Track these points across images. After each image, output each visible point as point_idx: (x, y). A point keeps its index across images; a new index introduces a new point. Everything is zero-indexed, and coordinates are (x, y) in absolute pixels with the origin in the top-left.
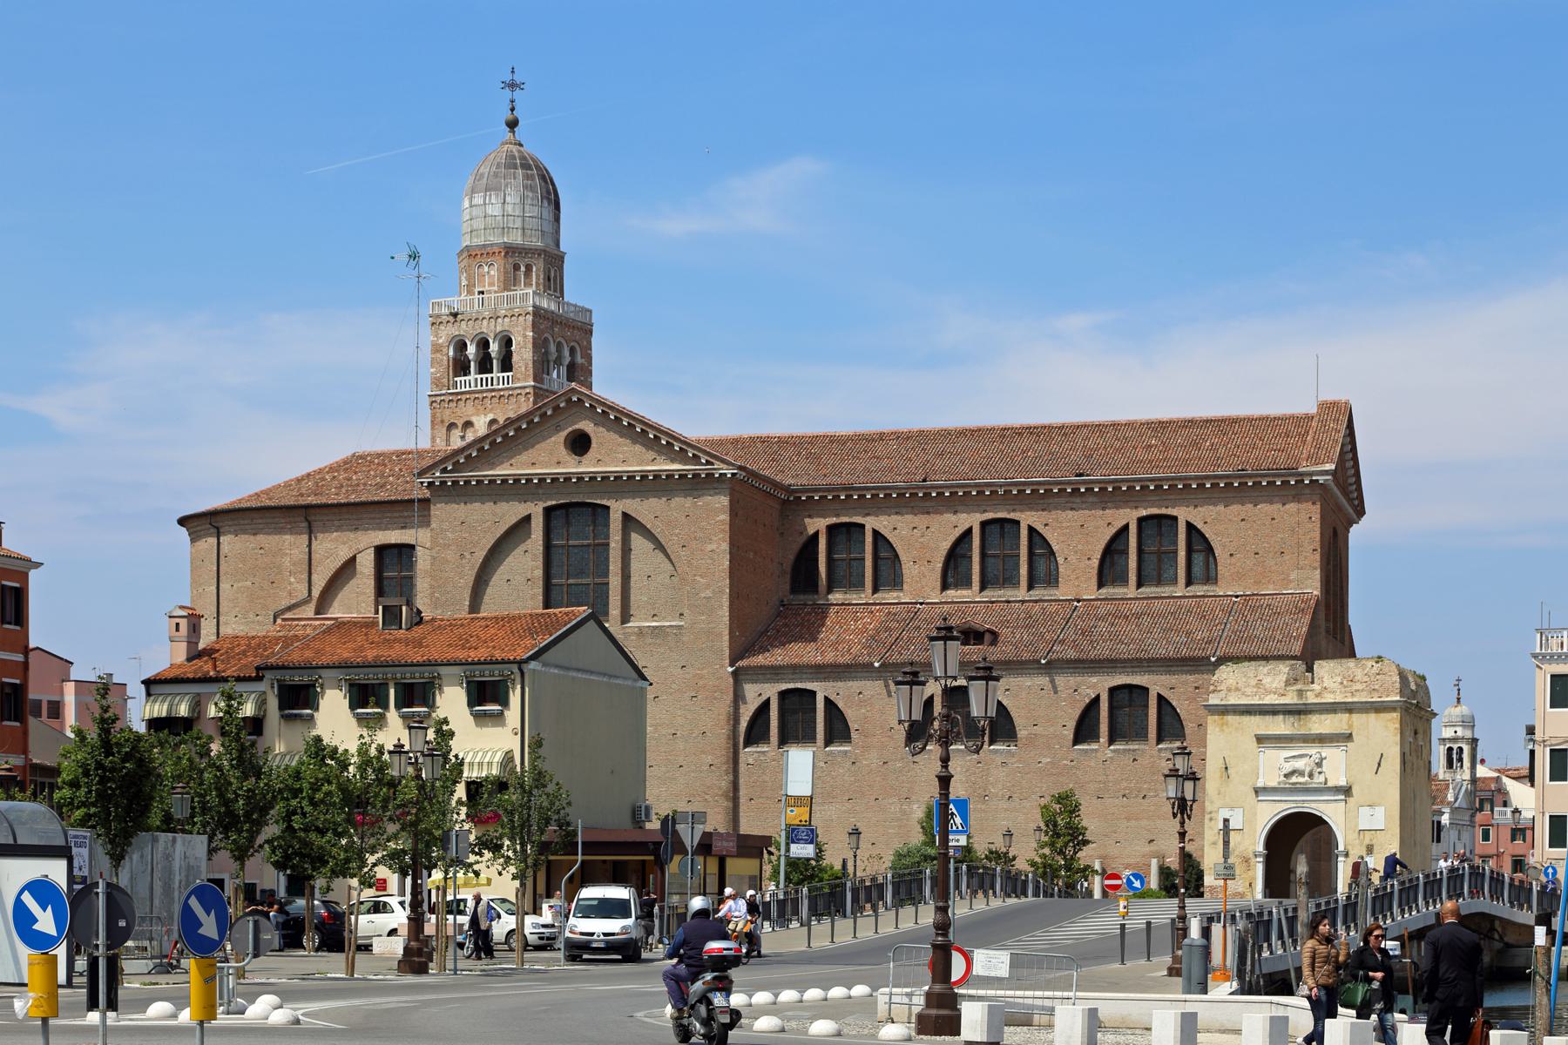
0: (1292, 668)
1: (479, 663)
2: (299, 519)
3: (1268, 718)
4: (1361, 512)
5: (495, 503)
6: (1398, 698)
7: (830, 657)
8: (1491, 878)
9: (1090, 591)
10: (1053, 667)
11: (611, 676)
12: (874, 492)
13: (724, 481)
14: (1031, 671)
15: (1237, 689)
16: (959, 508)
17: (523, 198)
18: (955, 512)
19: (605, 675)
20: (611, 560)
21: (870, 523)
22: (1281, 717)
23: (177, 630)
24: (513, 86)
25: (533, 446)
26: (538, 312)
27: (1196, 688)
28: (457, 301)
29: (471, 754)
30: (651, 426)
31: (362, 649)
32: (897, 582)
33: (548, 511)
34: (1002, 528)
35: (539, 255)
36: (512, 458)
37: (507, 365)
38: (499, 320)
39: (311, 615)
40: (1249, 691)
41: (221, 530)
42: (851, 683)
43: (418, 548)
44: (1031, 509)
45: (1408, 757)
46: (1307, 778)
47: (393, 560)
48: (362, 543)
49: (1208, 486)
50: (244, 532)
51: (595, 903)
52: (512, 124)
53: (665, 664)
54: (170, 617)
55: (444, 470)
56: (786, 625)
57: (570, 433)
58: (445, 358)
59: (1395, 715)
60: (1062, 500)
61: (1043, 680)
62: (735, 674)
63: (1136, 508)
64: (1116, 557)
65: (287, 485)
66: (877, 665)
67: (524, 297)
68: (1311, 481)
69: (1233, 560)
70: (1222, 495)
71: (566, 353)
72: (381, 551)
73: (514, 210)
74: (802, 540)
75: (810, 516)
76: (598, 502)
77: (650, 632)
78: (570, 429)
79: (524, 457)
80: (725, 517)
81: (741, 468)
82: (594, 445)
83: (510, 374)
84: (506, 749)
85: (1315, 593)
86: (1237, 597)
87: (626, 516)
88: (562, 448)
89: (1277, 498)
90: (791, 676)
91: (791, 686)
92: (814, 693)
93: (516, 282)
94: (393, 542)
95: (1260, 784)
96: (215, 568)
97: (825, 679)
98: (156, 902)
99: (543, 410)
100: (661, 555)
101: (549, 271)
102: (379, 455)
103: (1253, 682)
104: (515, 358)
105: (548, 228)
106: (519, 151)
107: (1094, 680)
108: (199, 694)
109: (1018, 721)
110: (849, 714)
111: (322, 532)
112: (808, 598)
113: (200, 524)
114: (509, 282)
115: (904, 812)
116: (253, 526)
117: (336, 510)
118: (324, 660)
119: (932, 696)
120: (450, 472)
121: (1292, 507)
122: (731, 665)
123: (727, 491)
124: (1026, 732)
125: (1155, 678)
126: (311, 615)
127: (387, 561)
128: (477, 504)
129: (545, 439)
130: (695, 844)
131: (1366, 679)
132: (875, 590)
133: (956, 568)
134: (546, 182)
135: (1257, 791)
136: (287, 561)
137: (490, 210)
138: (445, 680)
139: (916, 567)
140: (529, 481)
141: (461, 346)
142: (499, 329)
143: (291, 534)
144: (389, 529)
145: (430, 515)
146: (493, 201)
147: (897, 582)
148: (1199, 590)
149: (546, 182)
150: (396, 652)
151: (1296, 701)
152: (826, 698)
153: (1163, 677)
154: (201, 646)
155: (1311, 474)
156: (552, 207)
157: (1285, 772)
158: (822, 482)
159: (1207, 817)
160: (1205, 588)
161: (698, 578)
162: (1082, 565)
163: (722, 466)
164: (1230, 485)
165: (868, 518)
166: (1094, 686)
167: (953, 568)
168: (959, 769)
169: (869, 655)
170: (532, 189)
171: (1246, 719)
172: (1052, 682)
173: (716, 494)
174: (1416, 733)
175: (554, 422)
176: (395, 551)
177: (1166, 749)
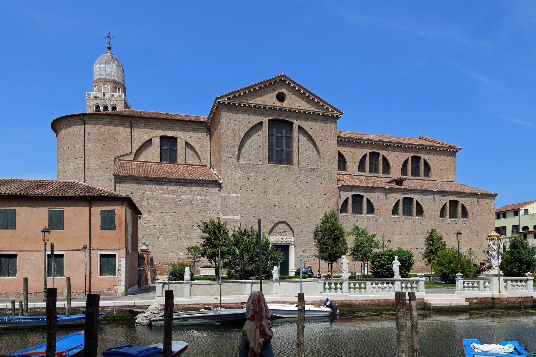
5: (248, 115)
14: (429, 194)
16: (363, 147)
18: (362, 148)
24: (109, 37)
25: (264, 96)
27: (472, 202)
28: (96, 94)
33: (269, 121)
35: (122, 86)
36: (255, 98)
39: (133, 160)
41: (86, 122)
42: (375, 194)
43: (178, 139)
44: (383, 150)
50: (100, 124)
53: (315, 182)
60: (392, 148)
61: (431, 197)
72: (162, 138)
73: (115, 71)
89: (445, 155)
90: (356, 190)
91: (356, 193)
93: (116, 92)
97: (367, 192)
107: (445, 198)
111: (137, 128)
114: (114, 91)
116: (104, 122)
117: (144, 120)
124: (427, 213)
125: (461, 198)
126: (133, 160)
128: (241, 115)
129: (268, 93)
136: (120, 138)
137: (107, 69)
142: (112, 103)
144: (166, 130)
152: (367, 198)
161: (326, 152)
167: (361, 167)
170: (120, 66)
172: (434, 198)
175: (273, 87)
176: (167, 139)
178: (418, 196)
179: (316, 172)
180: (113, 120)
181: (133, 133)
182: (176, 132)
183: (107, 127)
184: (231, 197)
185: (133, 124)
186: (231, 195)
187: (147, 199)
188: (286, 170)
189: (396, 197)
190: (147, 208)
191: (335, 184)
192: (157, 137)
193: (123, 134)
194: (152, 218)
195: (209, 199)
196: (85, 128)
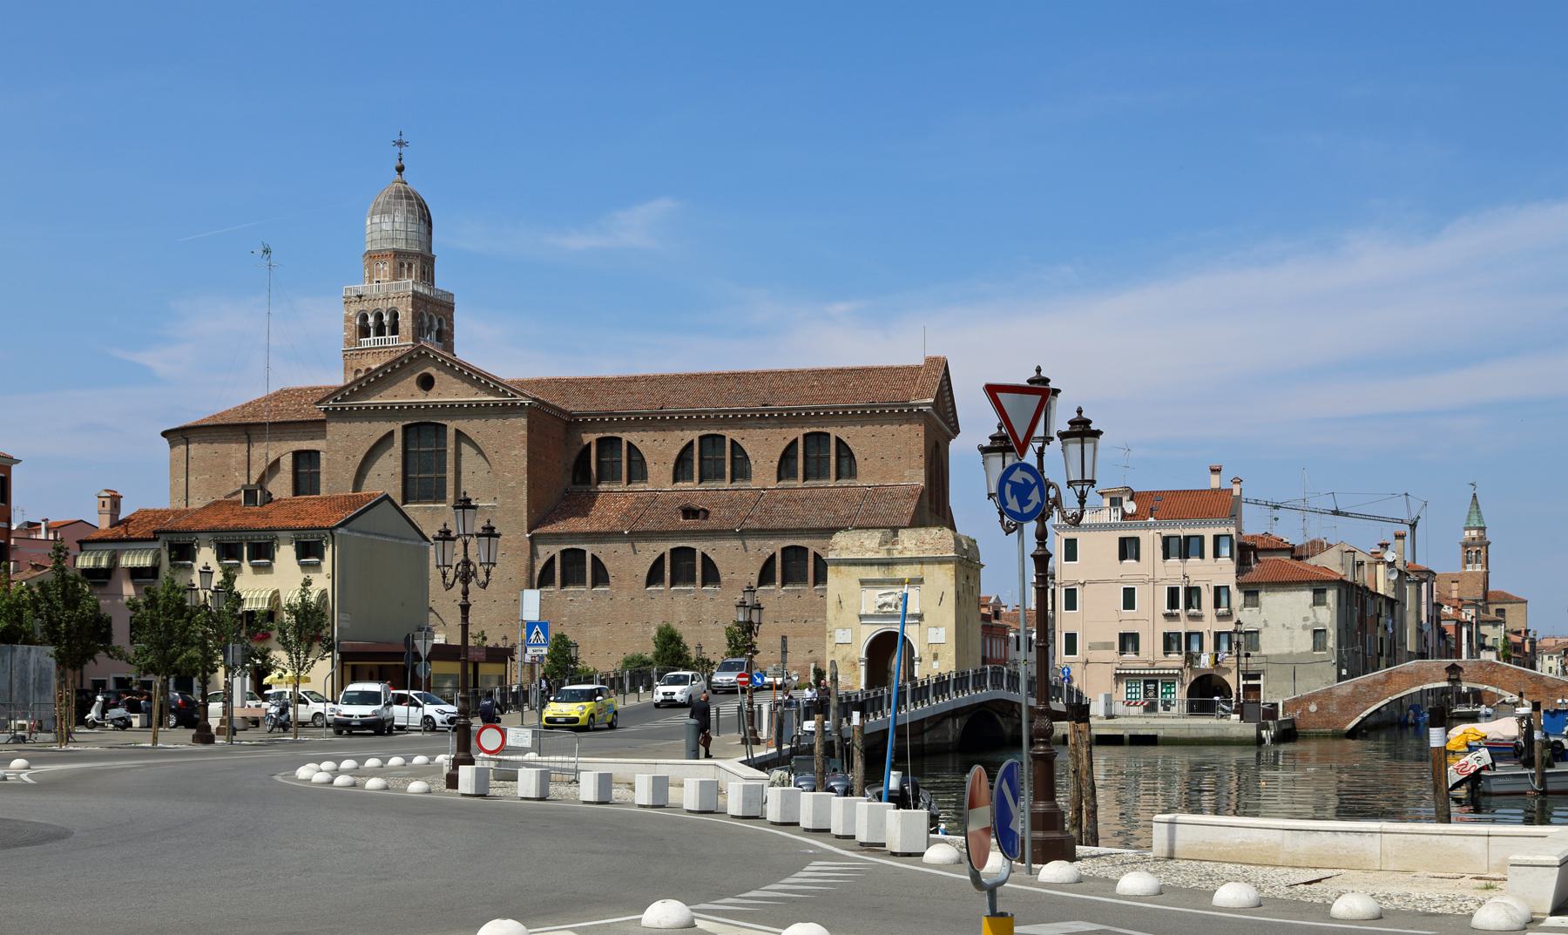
0: (884, 534)
1: (304, 529)
3: (868, 568)
4: (956, 431)
5: (370, 422)
6: (953, 554)
7: (595, 527)
8: (1008, 676)
9: (772, 483)
10: (744, 534)
11: (401, 539)
12: (627, 416)
15: (847, 549)
16: (684, 427)
17: (407, 218)
18: (682, 430)
19: (396, 537)
20: (448, 461)
21: (626, 437)
22: (876, 567)
23: (104, 506)
24: (400, 144)
25: (395, 384)
26: (415, 295)
28: (361, 287)
29: (245, 592)
30: (474, 371)
31: (227, 519)
32: (643, 477)
33: (405, 428)
34: (714, 441)
35: (417, 257)
37: (395, 330)
38: (390, 300)
40: (855, 549)
42: (609, 545)
44: (733, 428)
45: (961, 594)
46: (893, 609)
47: (306, 462)
48: (284, 450)
49: (850, 413)
51: (357, 694)
52: (400, 169)
54: (99, 497)
55: (335, 400)
56: (568, 506)
57: (421, 375)
58: (353, 326)
59: (951, 565)
60: (753, 422)
61: (738, 543)
62: (531, 538)
63: (803, 427)
64: (790, 460)
65: (235, 410)
66: (626, 532)
67: (406, 285)
68: (918, 410)
69: (867, 462)
71: (436, 323)
72: (297, 455)
74: (581, 447)
75: (585, 432)
76: (439, 422)
78: (420, 373)
79: (389, 392)
80: (524, 432)
81: (534, 399)
82: (436, 384)
83: (397, 336)
84: (322, 588)
85: (922, 484)
86: (870, 487)
87: (458, 432)
88: (415, 385)
91: (569, 547)
92: (584, 552)
93: (401, 275)
94: (305, 448)
95: (863, 612)
96: (185, 466)
98: (15, 694)
99: (402, 359)
100: (481, 458)
101: (424, 267)
102: (298, 390)
103: (858, 544)
104: (400, 326)
105: (423, 239)
106: (404, 188)
107: (772, 543)
108: (115, 550)
109: (721, 571)
110: (608, 565)
112: (584, 488)
113: (176, 436)
114: (397, 275)
115: (644, 632)
118: (200, 527)
119: (664, 554)
120: (339, 401)
121: (906, 427)
122: (529, 533)
123: (526, 415)
125: (812, 541)
127: (301, 461)
129: (403, 379)
130: (427, 654)
131: (932, 541)
132: (629, 482)
133: (683, 467)
134: (422, 208)
135: (861, 617)
136: (233, 462)
138: (281, 540)
140: (392, 407)
141: (364, 318)
142: (389, 306)
143: (236, 443)
145: (325, 431)
146: (387, 220)
147: (643, 477)
148: (844, 482)
149: (422, 208)
150: (251, 522)
151: (886, 556)
152: (592, 554)
153: (818, 541)
154: (121, 517)
155: (918, 405)
156: (426, 225)
157: (879, 604)
158: (593, 409)
159: (828, 635)
160: (849, 481)
162: (767, 466)
163: (522, 398)
164: (863, 412)
165: (624, 434)
166: (771, 547)
167: (681, 469)
169: (622, 526)
170: (412, 212)
171: (853, 569)
172: (744, 544)
173: (518, 417)
174: (968, 578)
177: (820, 589)
178: (705, 543)
179: (486, 512)
181: (251, 452)
182: (318, 442)
183: (216, 445)
185: (251, 436)
189: (655, 549)
191: (523, 533)
192: (288, 455)
196: (188, 449)
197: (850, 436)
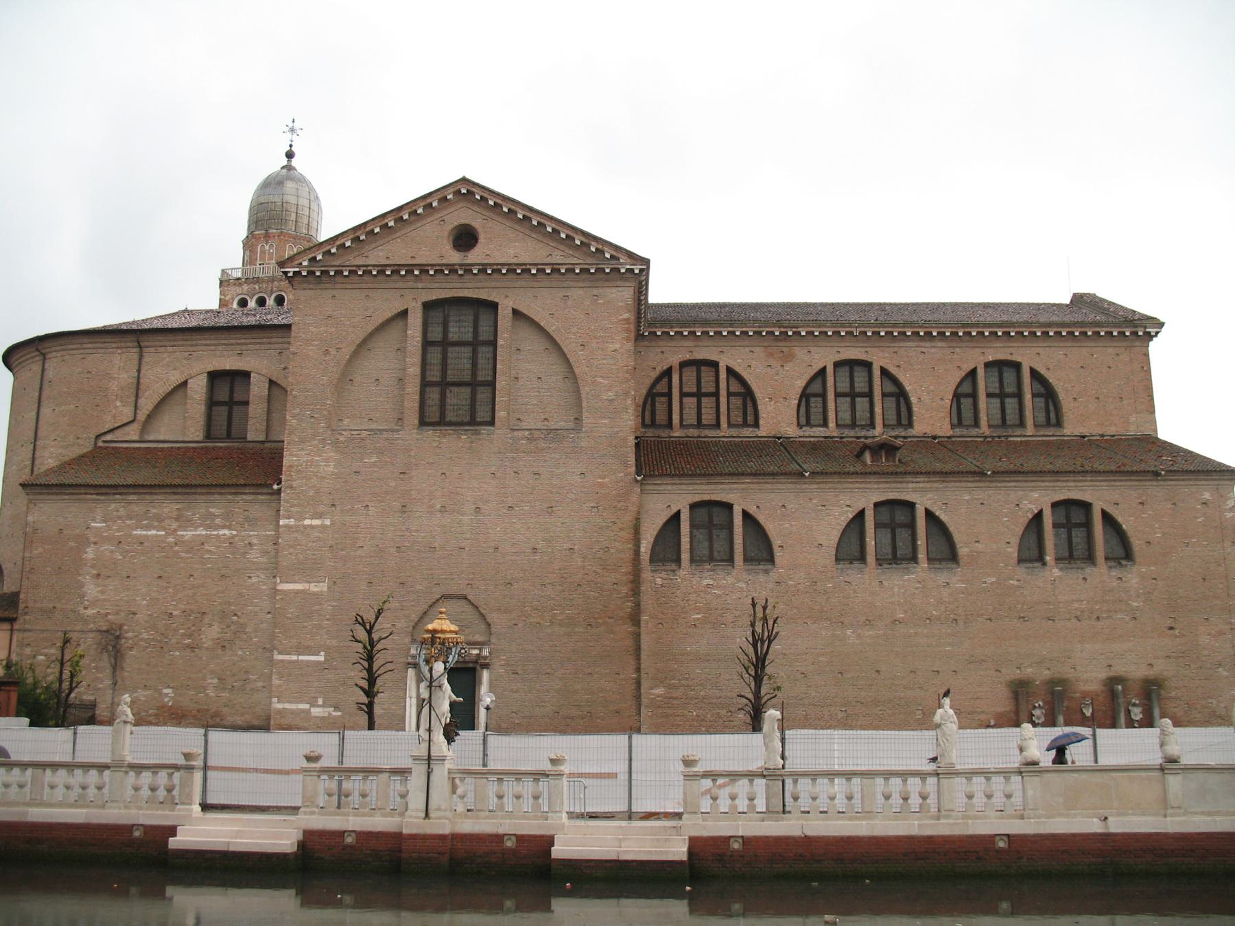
2: (130, 344)
13: (626, 280)
33: (428, 306)
39: (136, 438)
43: (252, 375)
70: (1061, 345)
77: (542, 436)
94: (228, 368)
110: (770, 527)
116: (82, 351)
136: (114, 386)
139: (772, 403)
161: (599, 380)
168: (896, 590)
180: (101, 345)
181: (143, 371)
184: (306, 527)
186: (307, 522)
187: (95, 543)
188: (472, 442)
190: (93, 566)
192: (201, 377)
193: (121, 376)
194: (103, 593)
195: (251, 536)
196: (43, 370)
197: (1051, 367)
